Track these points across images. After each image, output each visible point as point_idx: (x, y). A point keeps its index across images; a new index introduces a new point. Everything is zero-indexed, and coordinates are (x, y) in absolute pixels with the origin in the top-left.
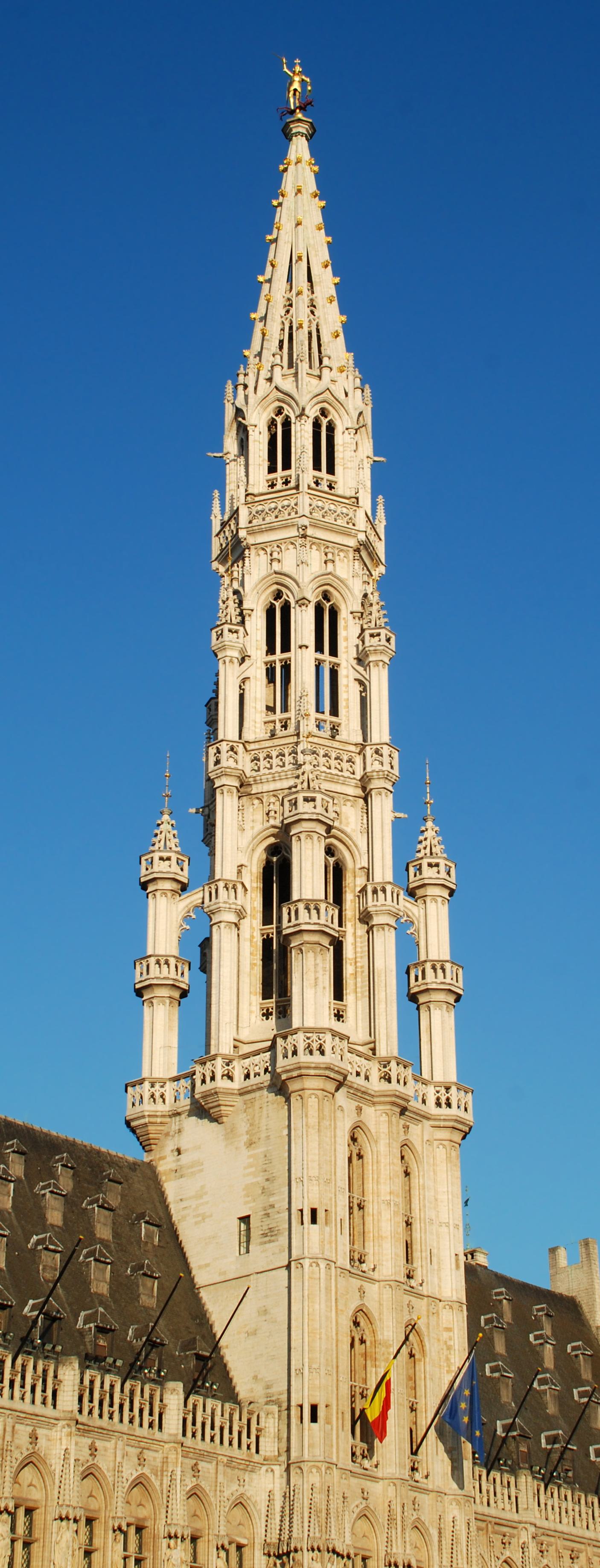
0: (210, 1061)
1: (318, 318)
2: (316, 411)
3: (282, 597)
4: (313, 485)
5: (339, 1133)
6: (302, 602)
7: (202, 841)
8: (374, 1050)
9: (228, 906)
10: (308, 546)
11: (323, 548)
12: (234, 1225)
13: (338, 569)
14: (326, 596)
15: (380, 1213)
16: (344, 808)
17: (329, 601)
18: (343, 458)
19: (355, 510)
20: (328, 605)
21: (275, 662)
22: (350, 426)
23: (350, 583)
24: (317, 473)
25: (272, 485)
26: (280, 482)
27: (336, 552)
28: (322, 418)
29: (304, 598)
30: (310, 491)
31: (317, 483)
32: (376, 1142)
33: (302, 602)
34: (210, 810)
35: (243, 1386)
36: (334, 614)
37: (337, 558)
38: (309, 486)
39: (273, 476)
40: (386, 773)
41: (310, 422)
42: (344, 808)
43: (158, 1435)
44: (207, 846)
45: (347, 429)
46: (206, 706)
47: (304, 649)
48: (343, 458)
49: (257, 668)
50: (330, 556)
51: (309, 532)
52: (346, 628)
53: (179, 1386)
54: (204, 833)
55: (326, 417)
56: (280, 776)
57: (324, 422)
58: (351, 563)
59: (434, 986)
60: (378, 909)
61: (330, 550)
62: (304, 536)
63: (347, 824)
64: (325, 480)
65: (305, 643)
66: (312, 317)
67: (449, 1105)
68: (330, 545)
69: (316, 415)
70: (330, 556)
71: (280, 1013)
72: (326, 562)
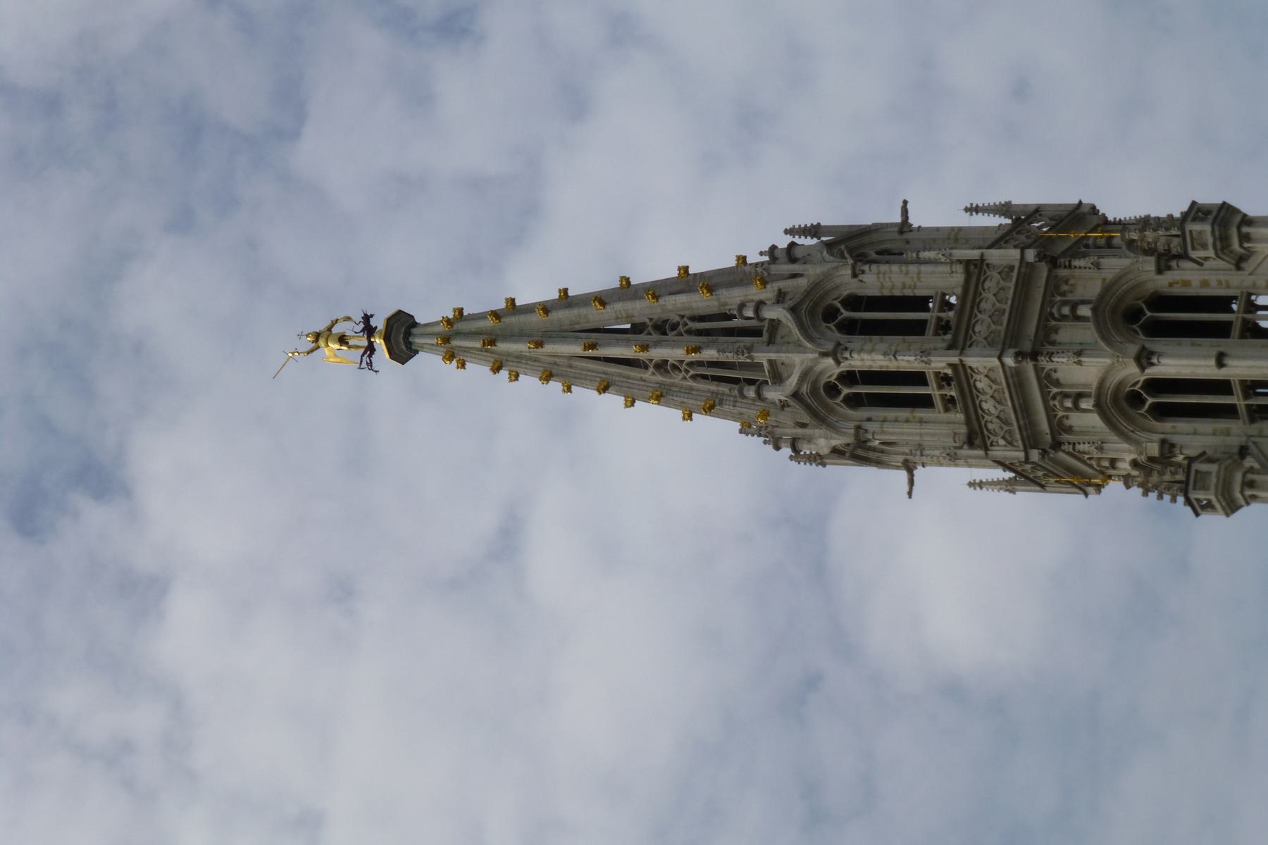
1: (682, 317)
2: (829, 328)
3: (1138, 392)
4: (949, 337)
11: (1054, 323)
13: (1087, 297)
14: (1132, 316)
17: (1140, 312)
19: (988, 265)
20: (1149, 314)
21: (1248, 406)
22: (849, 272)
23: (1109, 275)
24: (931, 329)
25: (952, 400)
27: (1058, 298)
30: (960, 344)
37: (1070, 297)
39: (938, 402)
45: (855, 275)
49: (1260, 436)
50: (1066, 310)
51: (1027, 346)
52: (1186, 284)
55: (838, 310)
57: (846, 314)
61: (1055, 311)
64: (942, 315)
66: (681, 329)
69: (834, 328)
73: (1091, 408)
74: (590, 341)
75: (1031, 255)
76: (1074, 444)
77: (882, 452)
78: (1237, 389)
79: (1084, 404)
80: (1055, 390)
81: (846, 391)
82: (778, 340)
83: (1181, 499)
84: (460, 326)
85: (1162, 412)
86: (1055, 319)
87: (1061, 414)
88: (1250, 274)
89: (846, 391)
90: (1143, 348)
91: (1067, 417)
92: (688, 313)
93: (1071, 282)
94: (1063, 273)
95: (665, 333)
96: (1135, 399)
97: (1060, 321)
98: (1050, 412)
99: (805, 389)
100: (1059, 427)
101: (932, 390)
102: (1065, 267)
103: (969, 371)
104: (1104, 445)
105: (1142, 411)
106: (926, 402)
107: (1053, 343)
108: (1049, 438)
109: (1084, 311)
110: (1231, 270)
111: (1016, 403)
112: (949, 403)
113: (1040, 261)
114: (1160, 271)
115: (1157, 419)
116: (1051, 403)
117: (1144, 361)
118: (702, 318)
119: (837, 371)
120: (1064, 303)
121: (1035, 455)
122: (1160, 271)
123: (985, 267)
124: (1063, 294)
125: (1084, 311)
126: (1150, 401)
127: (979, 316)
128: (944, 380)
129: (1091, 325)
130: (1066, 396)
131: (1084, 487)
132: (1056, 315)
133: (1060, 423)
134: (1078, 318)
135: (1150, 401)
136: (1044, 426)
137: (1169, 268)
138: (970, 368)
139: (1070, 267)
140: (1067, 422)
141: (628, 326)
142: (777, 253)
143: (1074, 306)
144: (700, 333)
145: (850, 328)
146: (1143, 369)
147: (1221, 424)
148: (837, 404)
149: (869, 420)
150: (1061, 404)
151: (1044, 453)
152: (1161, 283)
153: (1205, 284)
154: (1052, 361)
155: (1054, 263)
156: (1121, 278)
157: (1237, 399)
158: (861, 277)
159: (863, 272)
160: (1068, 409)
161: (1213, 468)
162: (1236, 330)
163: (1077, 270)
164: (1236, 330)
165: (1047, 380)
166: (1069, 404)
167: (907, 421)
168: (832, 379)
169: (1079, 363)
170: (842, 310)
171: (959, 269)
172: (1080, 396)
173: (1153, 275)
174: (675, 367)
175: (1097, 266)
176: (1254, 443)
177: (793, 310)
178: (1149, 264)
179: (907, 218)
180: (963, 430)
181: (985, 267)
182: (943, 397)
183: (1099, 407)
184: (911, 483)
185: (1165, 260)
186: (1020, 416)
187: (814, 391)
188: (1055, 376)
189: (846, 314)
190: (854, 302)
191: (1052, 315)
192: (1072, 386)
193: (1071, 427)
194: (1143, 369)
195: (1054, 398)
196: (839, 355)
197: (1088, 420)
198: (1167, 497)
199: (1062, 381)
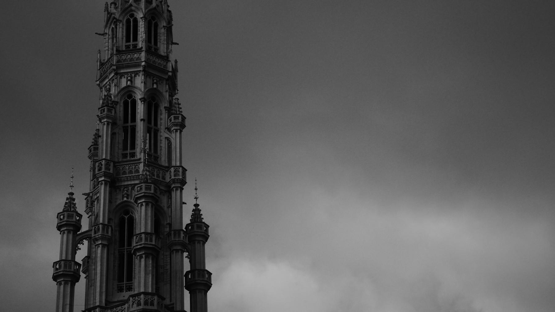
0: (93, 310)
7: (85, 211)
9: (104, 236)
18: (164, 36)
20: (154, 103)
22: (165, 25)
23: (164, 93)
34: (92, 194)
40: (181, 180)
44: (87, 214)
45: (164, 26)
46: (88, 149)
48: (164, 36)
49: (119, 129)
50: (155, 81)
52: (161, 114)
54: (86, 208)
56: (130, 178)
57: (153, 22)
59: (199, 282)
60: (177, 242)
61: (155, 78)
69: (150, 19)
71: (127, 289)
73: (128, 84)
75: (170, 74)
76: (117, 79)
77: (110, 28)
79: (129, 82)
80: (133, 75)
85: (126, 104)
86: (153, 78)
87: (126, 76)
88: (164, 131)
90: (146, 100)
91: (125, 78)
93: (162, 84)
94: (165, 82)
96: (130, 96)
97: (153, 79)
98: (127, 73)
99: (133, 8)
100: (122, 75)
101: (132, 43)
102: (166, 83)
103: (140, 53)
104: (117, 87)
105: (126, 98)
107: (147, 77)
108: (119, 72)
109: (155, 86)
110: (165, 126)
111: (130, 64)
112: (128, 47)
113: (168, 76)
114: (165, 107)
115: (124, 101)
116: (129, 74)
117: (143, 100)
121: (115, 67)
122: (165, 107)
123: (167, 61)
124: (159, 81)
125: (155, 86)
126: (130, 101)
127: (155, 58)
129: (152, 87)
130: (131, 78)
131: (99, 80)
132: (154, 78)
133: (123, 75)
136: (122, 71)
137: (166, 110)
138: (141, 53)
139: (166, 84)
140: (123, 77)
143: (156, 83)
146: (140, 99)
147: (122, 118)
148: (128, 16)
149: (123, 25)
150: (129, 76)
151: (114, 70)
152: (162, 108)
153: (161, 119)
154: (142, 75)
155: (167, 80)
157: (130, 124)
158: (163, 28)
159: (164, 29)
160: (127, 78)
161: (113, 114)
163: (165, 86)
165: (136, 73)
167: (123, 35)
169: (142, 82)
170: (154, 22)
171: (165, 54)
172: (131, 81)
175: (166, 91)
176: (117, 127)
177: (155, 8)
178: (167, 105)
179: (174, 44)
180: (120, 49)
181: (167, 61)
183: (127, 87)
186: (126, 65)
187: (132, 10)
188: (137, 76)
189: (153, 22)
191: (154, 77)
192: (134, 80)
193: (122, 78)
194: (140, 99)
195: (131, 74)
196: (144, 18)
197: (124, 83)
199: (136, 77)
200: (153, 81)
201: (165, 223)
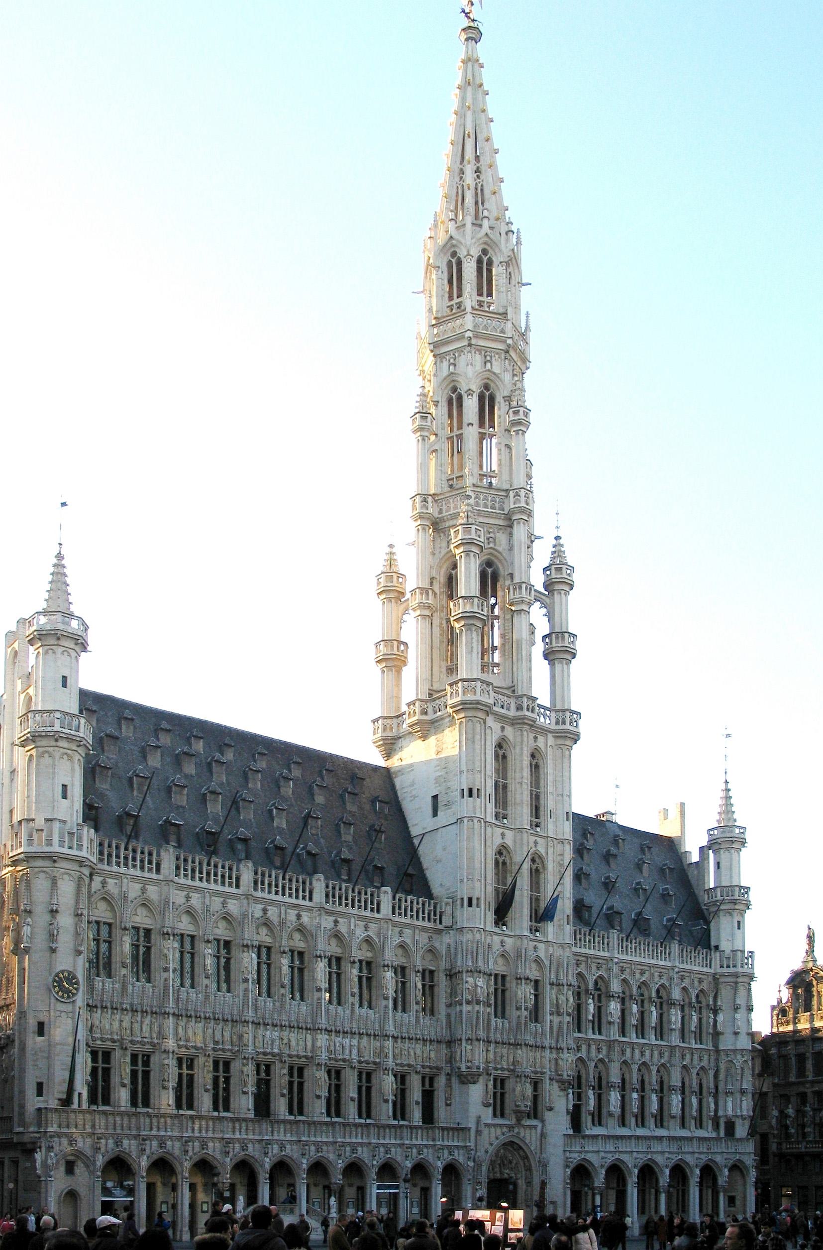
4: (477, 307)
5: (488, 743)
6: (470, 392)
8: (514, 691)
10: (473, 352)
11: (483, 353)
12: (429, 801)
13: (493, 367)
15: (516, 790)
16: (498, 535)
17: (488, 390)
20: (487, 394)
22: (502, 260)
23: (502, 376)
26: (455, 307)
28: (483, 256)
29: (470, 390)
30: (474, 312)
31: (481, 306)
32: (514, 748)
33: (470, 392)
35: (436, 890)
36: (492, 399)
37: (493, 359)
38: (472, 307)
41: (475, 259)
42: (498, 535)
43: (376, 915)
45: (501, 263)
47: (470, 427)
50: (488, 358)
51: (473, 341)
52: (499, 409)
53: (388, 889)
57: (485, 259)
58: (503, 362)
61: (488, 353)
62: (470, 345)
63: (500, 545)
65: (470, 421)
67: (564, 723)
68: (489, 350)
70: (488, 358)
72: (485, 363)
74: (471, 135)
75: (509, 341)
78: (460, 432)
81: (454, 261)
82: (474, 228)
83: (417, 410)
84: (476, 66)
87: (448, 358)
89: (454, 261)
92: (484, 184)
95: (476, 172)
99: (454, 242)
101: (456, 300)
106: (451, 298)
118: (482, 190)
119: (461, 256)
120: (491, 357)
128: (459, 305)
134: (485, 363)
135: (454, 396)
141: (478, 154)
142: (510, 225)
144: (476, 189)
145: (479, 261)
152: (499, 399)
156: (502, 382)
162: (482, 430)
164: (482, 430)
166: (452, 361)
168: (458, 255)
172: (455, 365)
173: (502, 395)
174: (461, 178)
178: (506, 394)
182: (453, 305)
184: (418, 293)
185: (508, 399)
187: (454, 246)
190: (490, 263)
191: (486, 352)
198: (418, 405)
200: (485, 357)
201: (506, 573)
